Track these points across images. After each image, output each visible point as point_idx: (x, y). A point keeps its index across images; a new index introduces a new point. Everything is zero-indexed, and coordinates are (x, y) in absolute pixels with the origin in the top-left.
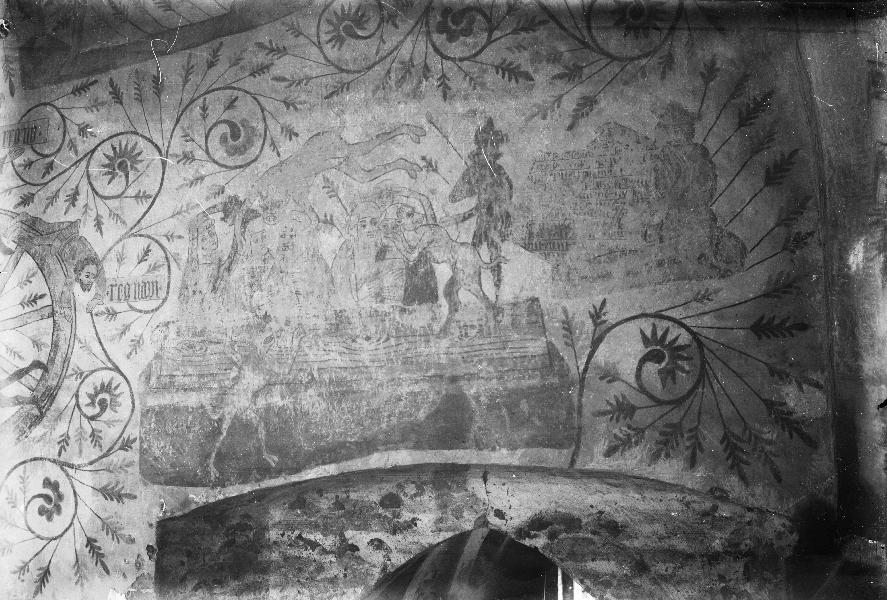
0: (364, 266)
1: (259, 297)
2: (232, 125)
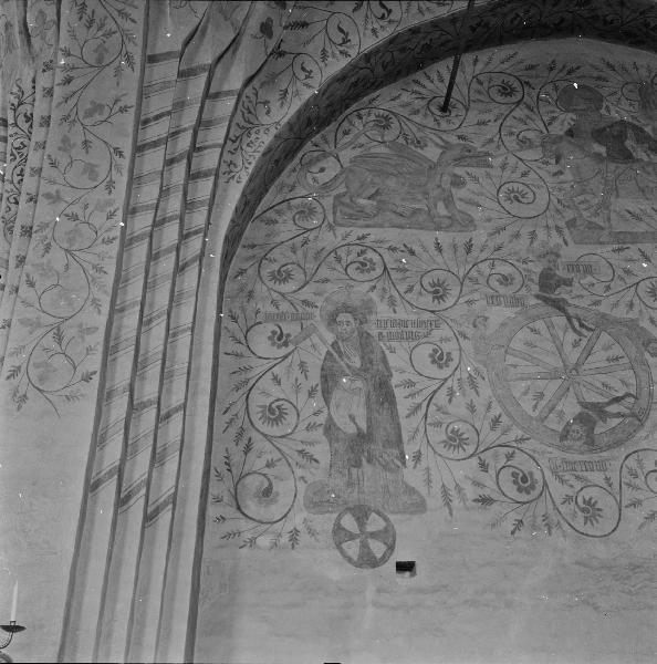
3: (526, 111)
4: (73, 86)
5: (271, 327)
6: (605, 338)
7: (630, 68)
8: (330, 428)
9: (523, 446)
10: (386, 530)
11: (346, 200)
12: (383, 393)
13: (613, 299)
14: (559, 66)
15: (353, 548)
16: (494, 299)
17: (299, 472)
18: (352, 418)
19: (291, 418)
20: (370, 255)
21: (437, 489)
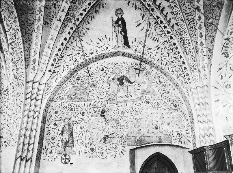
0: (151, 125)
1: (139, 128)
2: (136, 111)
3: (106, 75)
4: (14, 89)
5: (54, 122)
6: (111, 123)
7: (128, 63)
8: (62, 141)
9: (93, 143)
10: (69, 158)
11: (69, 96)
12: (71, 135)
13: (114, 115)
14: (114, 63)
15: (63, 161)
16: (92, 116)
17: (56, 148)
18: (66, 139)
19: (56, 139)
20: (72, 107)
21: (78, 151)
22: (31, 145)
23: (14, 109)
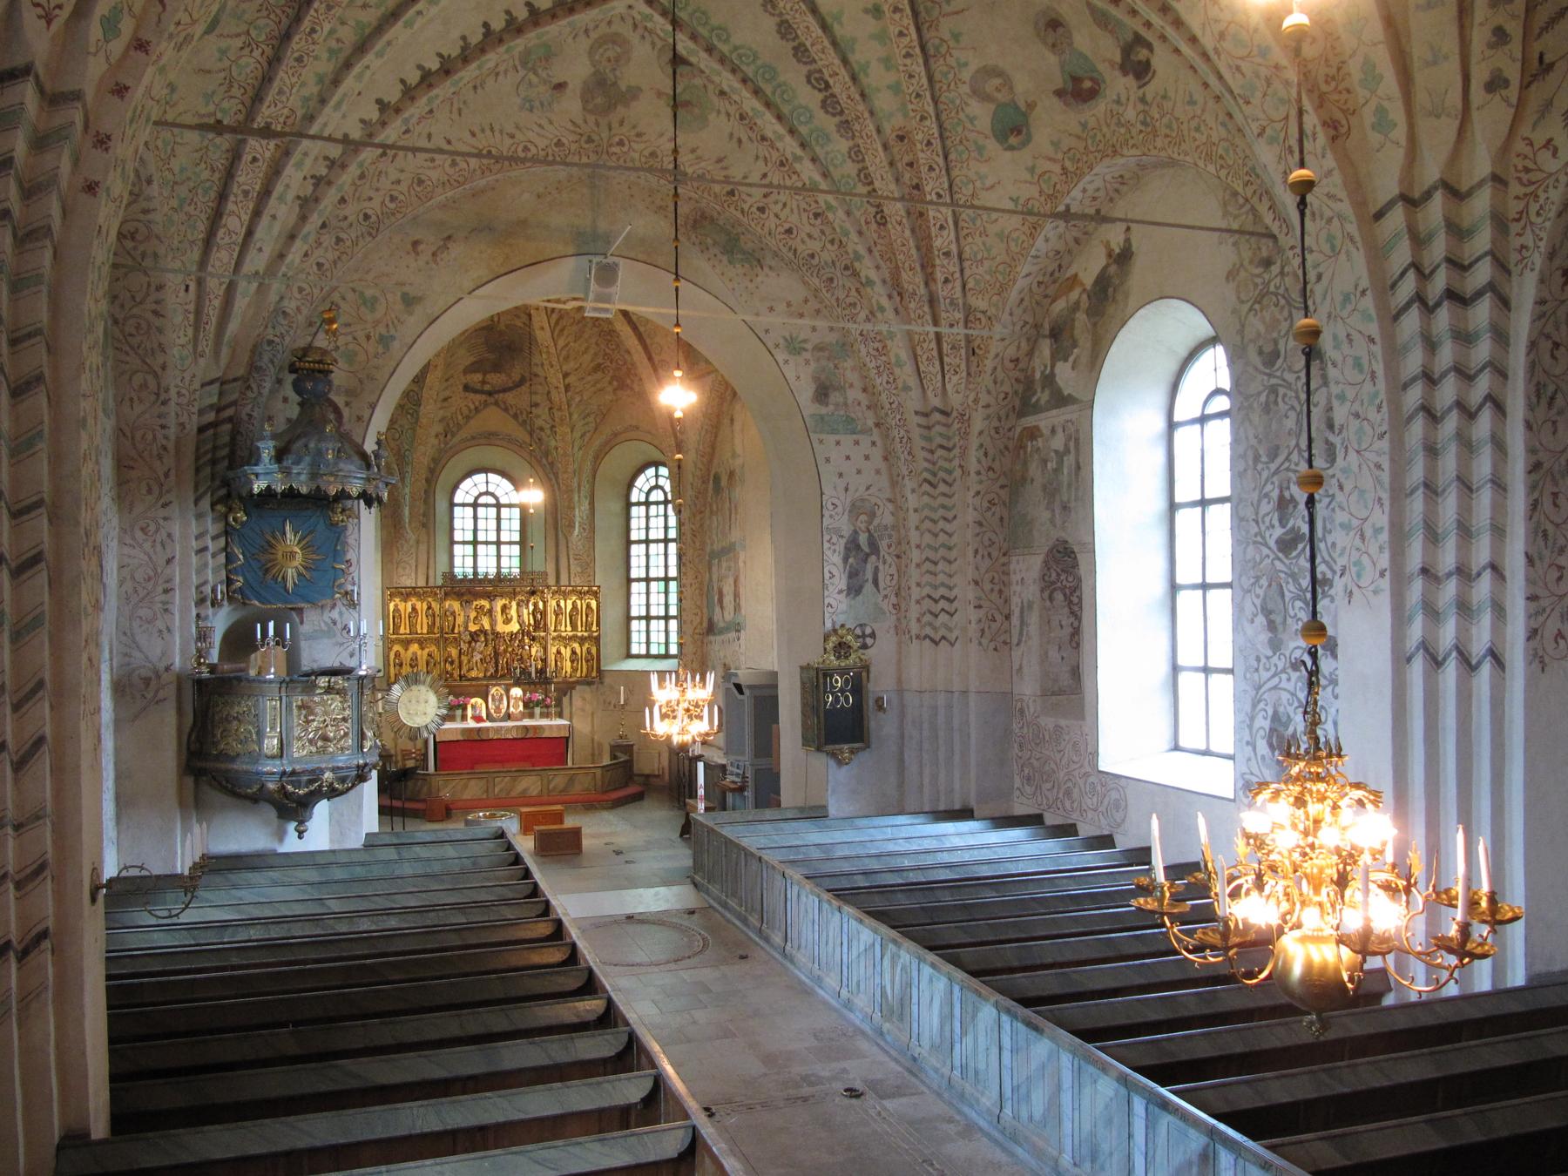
22: (1479, 575)
23: (1350, 394)
